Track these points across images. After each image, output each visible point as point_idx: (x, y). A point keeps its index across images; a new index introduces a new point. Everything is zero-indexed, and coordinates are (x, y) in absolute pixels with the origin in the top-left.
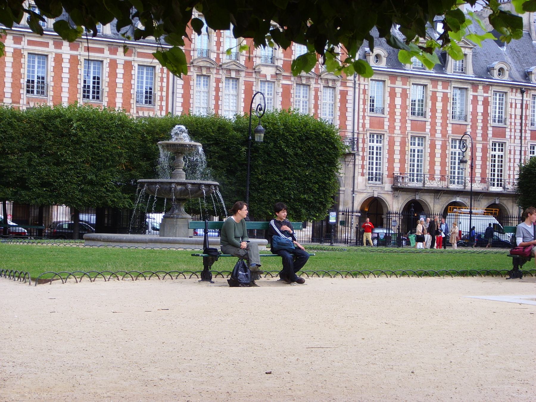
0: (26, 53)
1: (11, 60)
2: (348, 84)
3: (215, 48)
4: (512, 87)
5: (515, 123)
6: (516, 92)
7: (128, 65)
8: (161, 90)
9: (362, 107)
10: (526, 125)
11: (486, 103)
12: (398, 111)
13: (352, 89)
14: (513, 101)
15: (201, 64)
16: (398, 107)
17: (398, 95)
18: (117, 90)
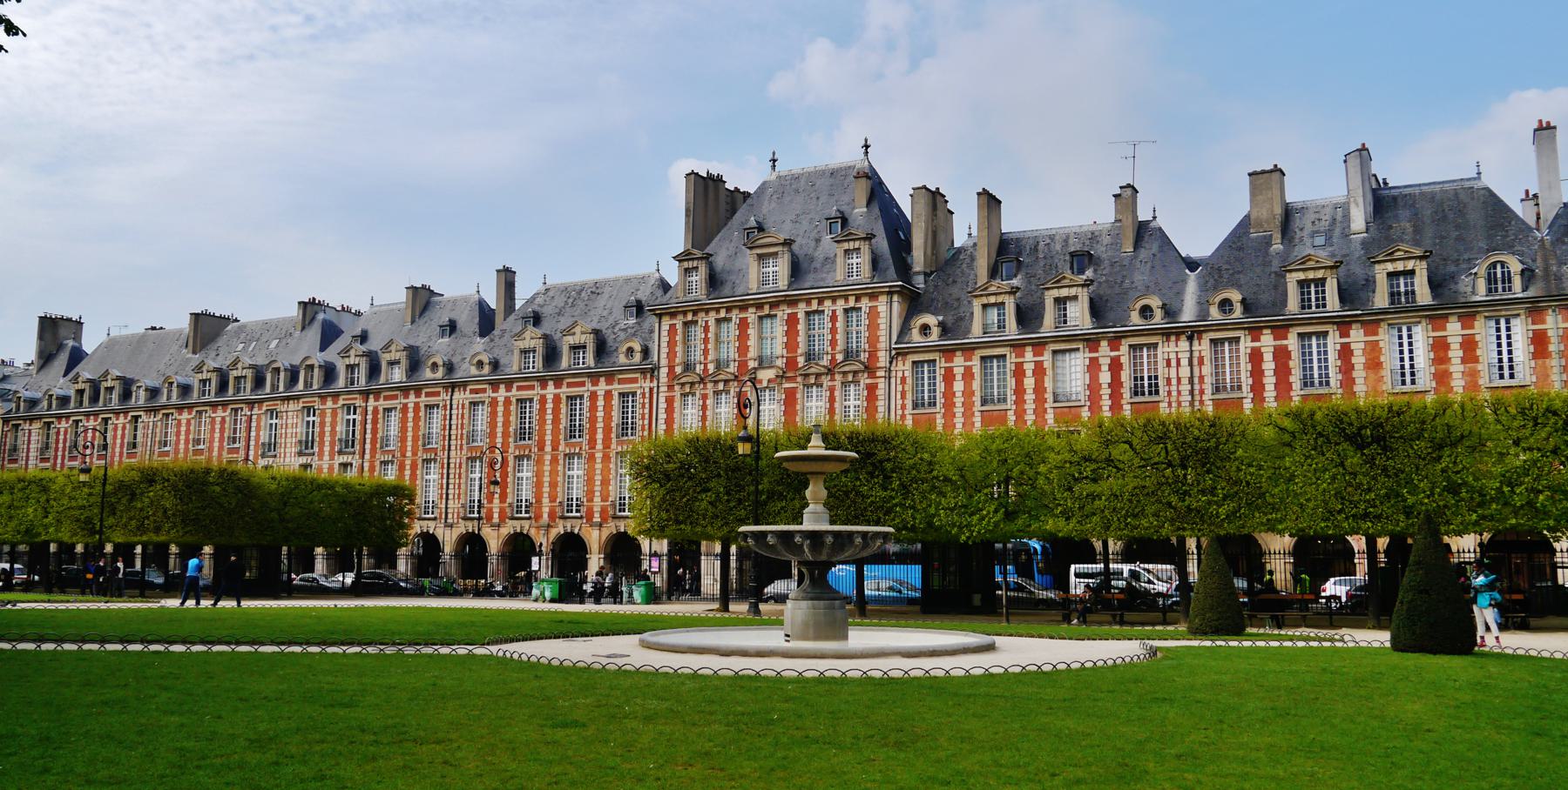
4: (1167, 334)
5: (1179, 393)
6: (1177, 340)
7: (608, 394)
9: (900, 402)
10: (1202, 392)
11: (1115, 366)
12: (959, 400)
14: (1173, 356)
16: (959, 394)
17: (959, 377)
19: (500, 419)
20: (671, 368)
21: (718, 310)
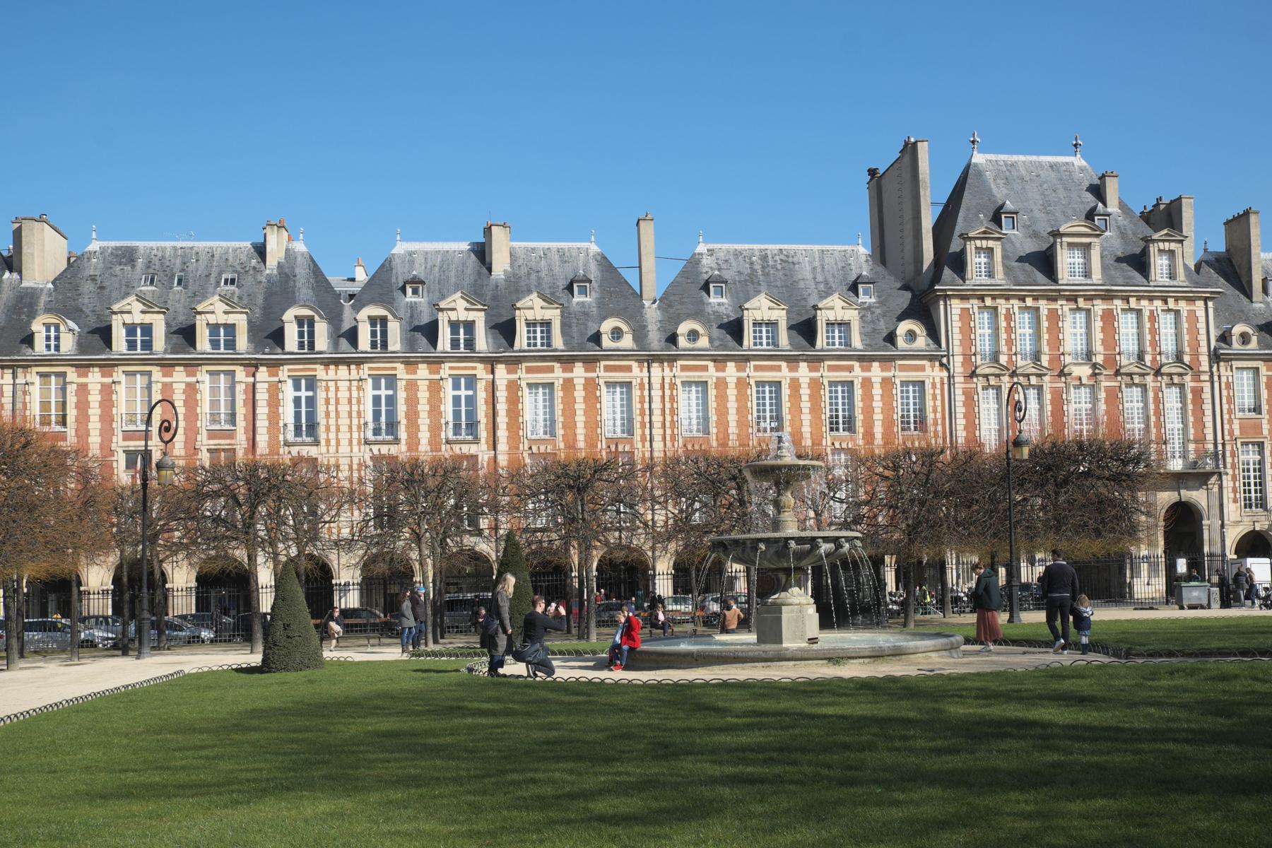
0: (752, 382)
1: (735, 392)
2: (1203, 378)
3: (1004, 349)
8: (935, 411)
13: (1208, 384)
15: (987, 371)
18: (875, 417)
19: (732, 405)
20: (967, 357)
21: (1023, 299)
